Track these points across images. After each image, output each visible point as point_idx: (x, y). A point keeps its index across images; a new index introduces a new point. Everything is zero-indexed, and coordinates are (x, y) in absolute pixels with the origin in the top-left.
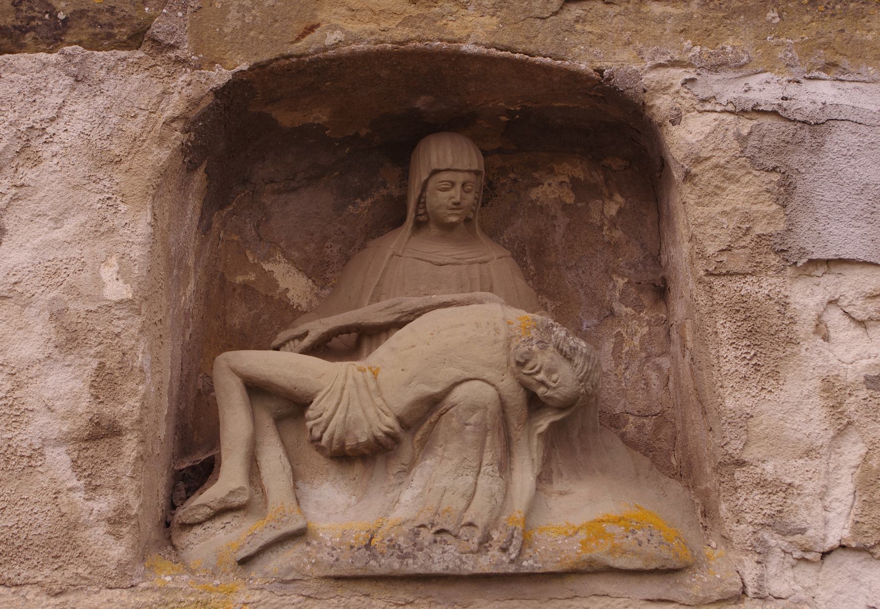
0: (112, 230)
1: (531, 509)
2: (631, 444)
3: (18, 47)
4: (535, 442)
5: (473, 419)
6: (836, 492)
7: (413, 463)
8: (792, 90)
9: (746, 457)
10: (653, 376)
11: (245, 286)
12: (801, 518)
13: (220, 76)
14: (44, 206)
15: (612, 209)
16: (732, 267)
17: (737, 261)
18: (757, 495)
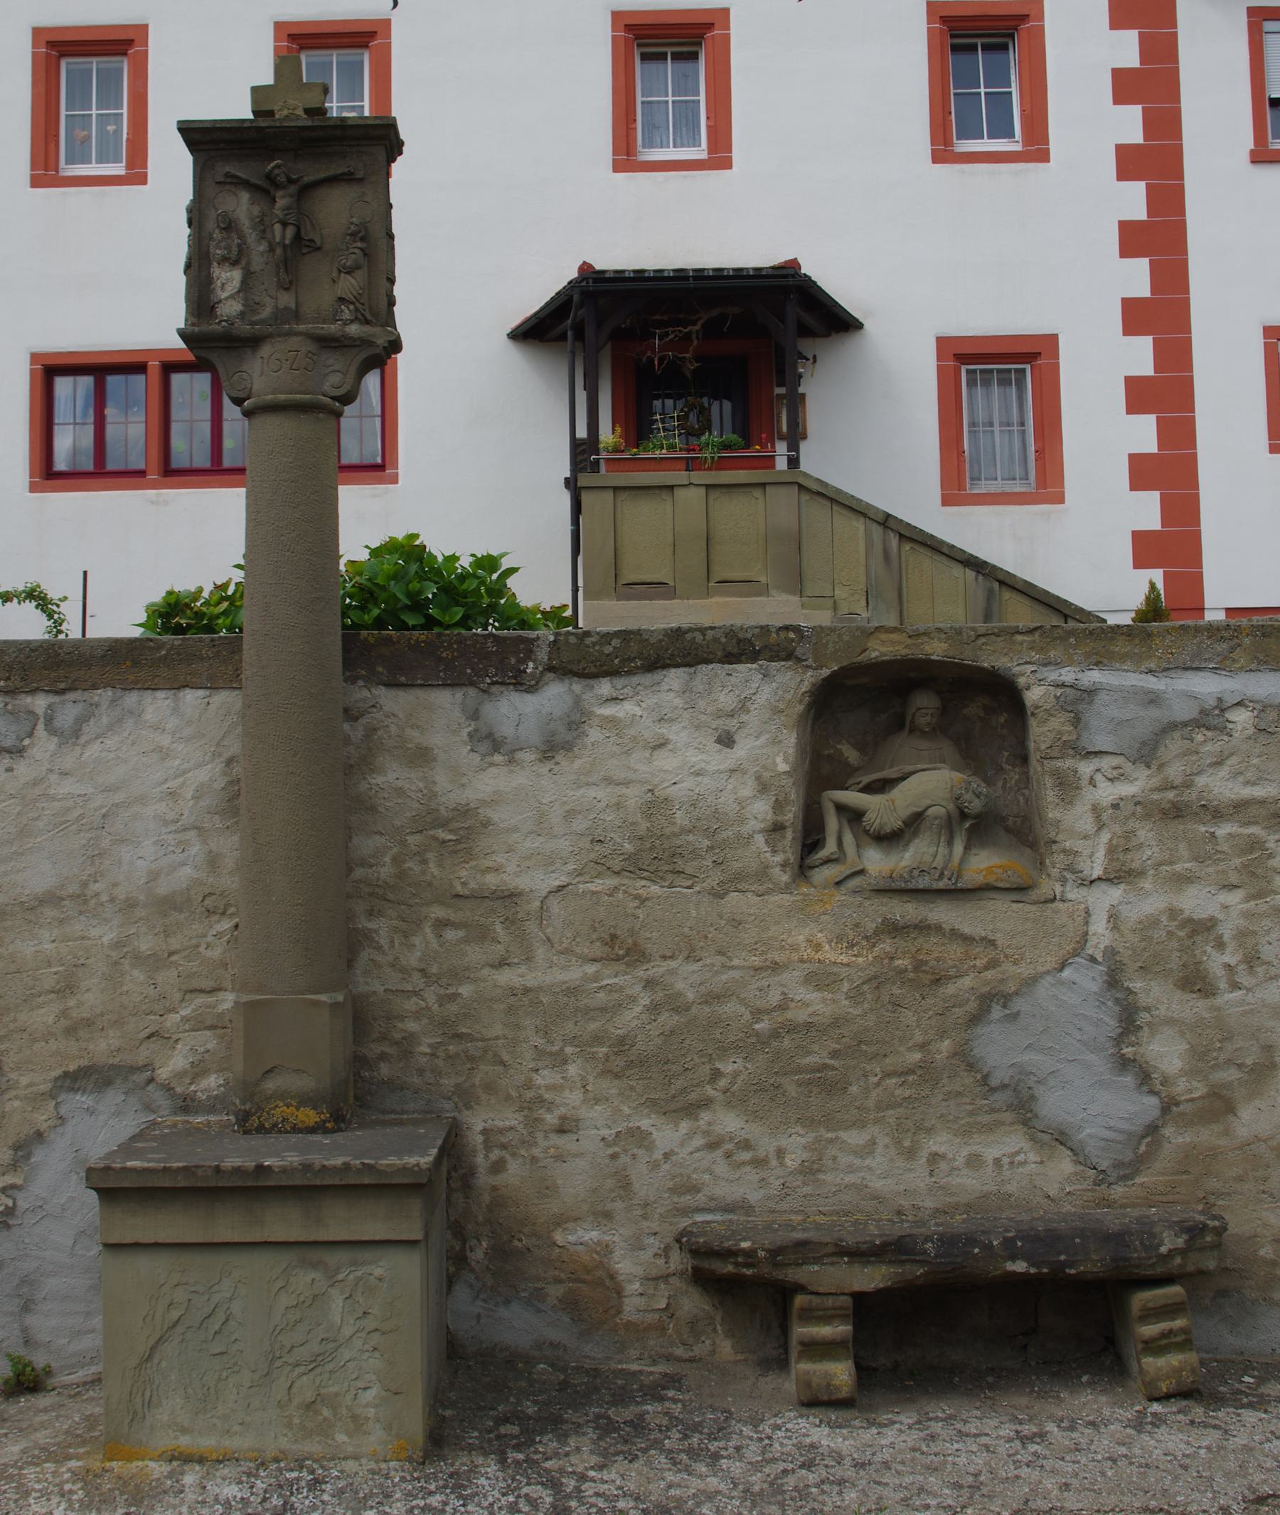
0: (780, 742)
1: (962, 861)
2: (1008, 830)
3: (739, 662)
4: (964, 832)
5: (936, 822)
6: (1097, 855)
7: (910, 841)
8: (1080, 675)
9: (1057, 839)
10: (1021, 798)
11: (829, 756)
13: (825, 672)
14: (752, 731)
15: (1002, 720)
16: (1052, 755)
17: (1055, 753)
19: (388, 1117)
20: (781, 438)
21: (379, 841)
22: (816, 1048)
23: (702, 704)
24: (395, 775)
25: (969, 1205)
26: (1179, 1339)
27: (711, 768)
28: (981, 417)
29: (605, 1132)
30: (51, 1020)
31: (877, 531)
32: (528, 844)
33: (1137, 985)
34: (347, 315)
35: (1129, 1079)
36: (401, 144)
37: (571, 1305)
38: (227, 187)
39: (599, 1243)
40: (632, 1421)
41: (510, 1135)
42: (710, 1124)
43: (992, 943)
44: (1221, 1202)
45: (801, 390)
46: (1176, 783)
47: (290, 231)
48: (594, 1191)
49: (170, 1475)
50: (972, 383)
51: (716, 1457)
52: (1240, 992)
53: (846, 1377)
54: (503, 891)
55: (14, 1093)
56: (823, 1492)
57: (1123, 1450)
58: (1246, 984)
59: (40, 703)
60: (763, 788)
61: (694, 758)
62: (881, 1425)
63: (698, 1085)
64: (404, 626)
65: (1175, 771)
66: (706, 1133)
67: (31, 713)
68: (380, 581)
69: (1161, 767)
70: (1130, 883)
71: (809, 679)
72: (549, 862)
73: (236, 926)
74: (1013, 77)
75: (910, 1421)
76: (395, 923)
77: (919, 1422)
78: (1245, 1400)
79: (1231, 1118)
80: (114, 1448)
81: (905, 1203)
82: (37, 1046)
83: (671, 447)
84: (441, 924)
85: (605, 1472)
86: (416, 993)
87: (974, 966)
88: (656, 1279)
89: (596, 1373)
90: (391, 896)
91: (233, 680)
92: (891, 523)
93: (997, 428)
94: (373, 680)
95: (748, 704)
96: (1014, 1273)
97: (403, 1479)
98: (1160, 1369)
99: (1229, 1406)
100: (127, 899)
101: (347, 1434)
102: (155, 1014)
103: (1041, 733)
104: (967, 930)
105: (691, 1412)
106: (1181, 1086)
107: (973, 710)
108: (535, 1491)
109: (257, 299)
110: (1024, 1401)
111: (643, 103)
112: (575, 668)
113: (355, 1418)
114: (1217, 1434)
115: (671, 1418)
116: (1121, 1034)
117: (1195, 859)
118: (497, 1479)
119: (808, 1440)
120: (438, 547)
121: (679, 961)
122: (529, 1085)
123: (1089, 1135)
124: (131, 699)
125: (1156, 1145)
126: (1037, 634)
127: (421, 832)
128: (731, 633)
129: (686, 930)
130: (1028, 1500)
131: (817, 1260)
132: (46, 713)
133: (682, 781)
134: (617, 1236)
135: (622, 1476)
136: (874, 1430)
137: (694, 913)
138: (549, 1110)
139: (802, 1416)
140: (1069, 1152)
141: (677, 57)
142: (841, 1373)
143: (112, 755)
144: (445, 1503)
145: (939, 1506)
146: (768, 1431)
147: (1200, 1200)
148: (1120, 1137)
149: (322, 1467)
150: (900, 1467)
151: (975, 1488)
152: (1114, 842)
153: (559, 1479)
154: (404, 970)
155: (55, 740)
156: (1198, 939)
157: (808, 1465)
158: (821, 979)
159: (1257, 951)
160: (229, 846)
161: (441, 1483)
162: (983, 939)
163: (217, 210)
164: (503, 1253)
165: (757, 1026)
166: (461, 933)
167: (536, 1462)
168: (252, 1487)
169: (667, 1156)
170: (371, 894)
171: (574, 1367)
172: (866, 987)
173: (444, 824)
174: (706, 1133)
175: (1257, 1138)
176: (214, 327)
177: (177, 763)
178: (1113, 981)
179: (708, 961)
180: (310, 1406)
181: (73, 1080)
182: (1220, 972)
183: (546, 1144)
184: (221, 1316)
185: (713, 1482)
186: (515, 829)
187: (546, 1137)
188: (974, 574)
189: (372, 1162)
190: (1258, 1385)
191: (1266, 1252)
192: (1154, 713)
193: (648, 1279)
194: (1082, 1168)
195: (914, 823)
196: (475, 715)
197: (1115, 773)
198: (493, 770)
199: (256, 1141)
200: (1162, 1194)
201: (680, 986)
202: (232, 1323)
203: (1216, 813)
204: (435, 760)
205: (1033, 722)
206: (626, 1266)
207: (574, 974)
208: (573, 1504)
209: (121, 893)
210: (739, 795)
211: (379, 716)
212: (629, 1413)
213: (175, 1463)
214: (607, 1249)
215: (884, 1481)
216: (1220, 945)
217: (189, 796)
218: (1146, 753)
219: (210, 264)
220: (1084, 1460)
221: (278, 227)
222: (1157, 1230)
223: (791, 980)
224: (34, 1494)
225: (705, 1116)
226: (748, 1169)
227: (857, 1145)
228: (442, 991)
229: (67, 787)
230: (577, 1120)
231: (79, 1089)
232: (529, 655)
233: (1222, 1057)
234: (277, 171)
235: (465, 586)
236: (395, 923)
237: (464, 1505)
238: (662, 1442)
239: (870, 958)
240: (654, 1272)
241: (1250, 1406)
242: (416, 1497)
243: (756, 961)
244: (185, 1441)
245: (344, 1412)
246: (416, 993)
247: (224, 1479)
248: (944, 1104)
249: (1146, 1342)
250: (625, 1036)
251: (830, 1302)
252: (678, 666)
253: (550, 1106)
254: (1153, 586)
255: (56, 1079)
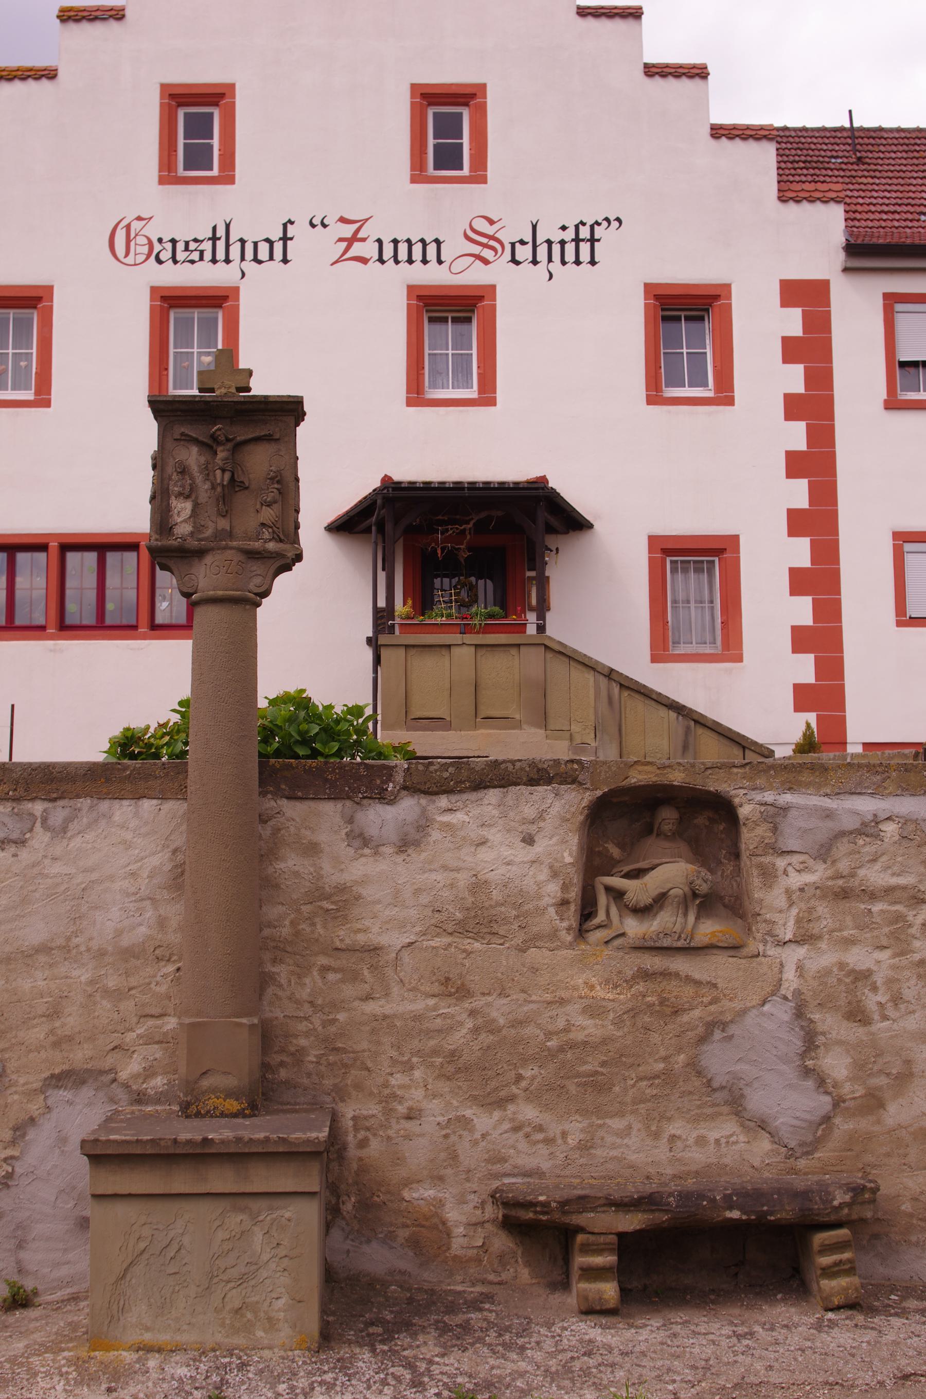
0: (567, 841)
2: (725, 906)
3: (538, 785)
4: (695, 907)
5: (676, 900)
6: (789, 924)
7: (657, 913)
8: (778, 797)
9: (761, 913)
10: (734, 884)
11: (599, 852)
12: (777, 932)
13: (599, 793)
14: (547, 834)
15: (721, 828)
16: (757, 853)
17: (759, 851)
18: (764, 925)
19: (285, 1107)
20: (531, 609)
21: (281, 909)
22: (590, 1059)
23: (512, 814)
24: (293, 862)
25: (697, 1172)
26: (846, 1267)
27: (517, 860)
28: (681, 596)
29: (440, 1119)
30: (42, 1036)
31: (603, 681)
32: (387, 913)
33: (816, 1016)
34: (267, 535)
35: (810, 1084)
36: (304, 414)
37: (414, 1243)
38: (182, 443)
39: (435, 1199)
40: (461, 1325)
41: (372, 1121)
42: (514, 1113)
43: (715, 986)
44: (875, 1172)
45: (547, 574)
46: (844, 874)
47: (227, 476)
48: (432, 1161)
49: (138, 1360)
50: (674, 570)
51: (523, 1348)
52: (888, 1022)
53: (612, 1293)
54: (369, 946)
55: (14, 1089)
56: (601, 1372)
57: (809, 1344)
58: (892, 1016)
59: (38, 808)
60: (555, 874)
61: (506, 853)
62: (637, 1327)
63: (506, 1086)
64: (297, 756)
65: (844, 866)
66: (512, 1120)
67: (31, 814)
68: (279, 723)
69: (834, 862)
70: (811, 944)
71: (588, 797)
72: (402, 926)
73: (178, 969)
74: (708, 341)
75: (658, 1325)
76: (292, 968)
77: (664, 1325)
78: (892, 1311)
79: (881, 1111)
80: (97, 1341)
81: (652, 1170)
82: (31, 1056)
83: (449, 616)
84: (325, 969)
85: (446, 1358)
86: (306, 1019)
87: (702, 1002)
88: (475, 1224)
89: (432, 1292)
90: (289, 949)
91: (181, 793)
92: (614, 676)
93: (692, 605)
94: (278, 794)
95: (544, 815)
96: (731, 1219)
97: (304, 1363)
98: (832, 1288)
99: (881, 1315)
100: (99, 950)
101: (264, 1331)
102: (118, 1032)
103: (749, 838)
104: (697, 976)
105: (502, 1319)
106: (846, 1089)
107: (701, 820)
108: (399, 1371)
109: (202, 523)
110: (737, 1311)
111: (429, 354)
112: (423, 788)
113: (269, 1319)
114: (874, 1334)
115: (488, 1323)
116: (805, 1051)
117: (857, 928)
118: (371, 1362)
119: (587, 1337)
120: (320, 699)
121: (494, 997)
122: (386, 1085)
123: (782, 1123)
124: (104, 805)
125: (829, 1131)
126: (748, 767)
127: (311, 903)
128: (533, 764)
129: (499, 975)
130: (743, 1378)
131: (593, 1209)
132: (42, 816)
133: (497, 869)
134: (448, 1194)
135: (458, 1361)
136: (633, 1331)
137: (504, 963)
138: (400, 1103)
139: (581, 1321)
140: (767, 1135)
141: (455, 320)
142: (609, 1290)
143: (90, 846)
144: (336, 1379)
145: (682, 1381)
146: (559, 1331)
147: (860, 1170)
148: (804, 1125)
149: (247, 1355)
150: (653, 1355)
151: (707, 1368)
152: (801, 915)
153: (414, 1363)
154: (298, 1002)
155: (49, 834)
156: (860, 984)
157: (589, 1354)
158: (594, 1010)
159: (900, 993)
160: (175, 912)
161: (332, 1365)
162: (708, 983)
163: (175, 459)
164: (365, 1205)
165: (549, 1044)
166: (339, 976)
167: (397, 1351)
168: (197, 1369)
169: (484, 1136)
170: (275, 947)
171: (416, 1289)
172: (625, 1016)
173: (328, 897)
174: (512, 1120)
175: (900, 1126)
176: (172, 542)
177: (137, 851)
178: (799, 1013)
179: (514, 997)
180: (237, 1311)
181: (58, 1080)
182: (874, 1008)
183: (398, 1127)
184: (175, 1247)
185: (523, 1365)
186: (379, 902)
187: (398, 1122)
188: (675, 715)
189: (285, 1136)
190: (901, 1302)
191: (906, 1207)
192: (830, 824)
193: (469, 1225)
194: (777, 1146)
195: (661, 900)
196: (351, 821)
197: (802, 866)
198: (363, 860)
199: (196, 1122)
200: (833, 1165)
201: (494, 1014)
202: (183, 1251)
203: (873, 896)
204: (322, 852)
205: (744, 830)
206: (454, 1215)
207: (419, 1005)
208: (426, 1379)
209: (95, 945)
210: (537, 879)
211: (282, 820)
212: (459, 1319)
213: (141, 1353)
214: (441, 1203)
215: (643, 1364)
216: (874, 989)
217: (145, 876)
218: (824, 853)
219: (169, 497)
220: (781, 1350)
221: (218, 472)
222: (831, 1189)
223: (573, 1009)
224: (40, 1375)
225: (511, 1108)
226: (540, 1146)
227: (619, 1129)
228: (325, 1017)
229: (57, 869)
230: (420, 1110)
231: (62, 1086)
232: (390, 778)
233: (875, 1068)
234: (219, 433)
235: (339, 727)
236: (292, 968)
237: (349, 1380)
238: (484, 1339)
239: (629, 996)
240: (474, 1220)
241: (896, 1315)
242: (314, 1375)
243: (548, 997)
244: (148, 1337)
245: (262, 1315)
246: (306, 1019)
247: (177, 1363)
248: (680, 1100)
249: (823, 1269)
250: (455, 1050)
251: (602, 1239)
252: (495, 787)
253: (401, 1100)
254: (808, 725)
255: (46, 1079)
